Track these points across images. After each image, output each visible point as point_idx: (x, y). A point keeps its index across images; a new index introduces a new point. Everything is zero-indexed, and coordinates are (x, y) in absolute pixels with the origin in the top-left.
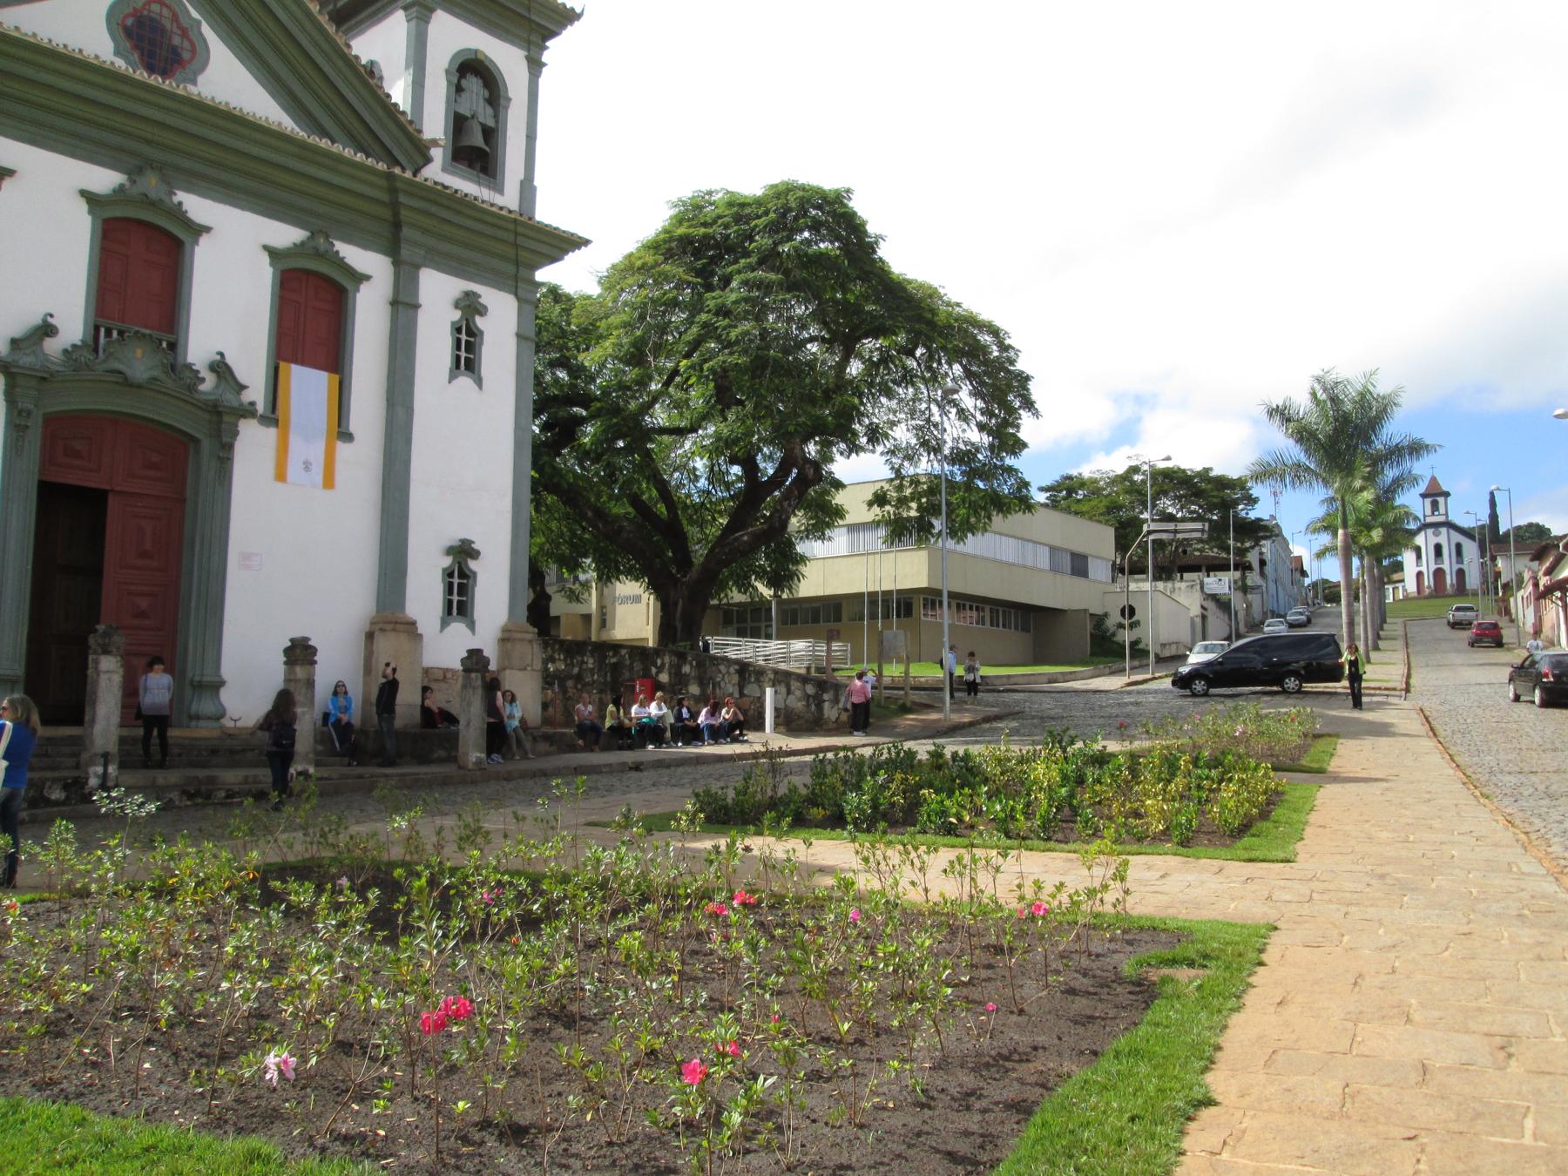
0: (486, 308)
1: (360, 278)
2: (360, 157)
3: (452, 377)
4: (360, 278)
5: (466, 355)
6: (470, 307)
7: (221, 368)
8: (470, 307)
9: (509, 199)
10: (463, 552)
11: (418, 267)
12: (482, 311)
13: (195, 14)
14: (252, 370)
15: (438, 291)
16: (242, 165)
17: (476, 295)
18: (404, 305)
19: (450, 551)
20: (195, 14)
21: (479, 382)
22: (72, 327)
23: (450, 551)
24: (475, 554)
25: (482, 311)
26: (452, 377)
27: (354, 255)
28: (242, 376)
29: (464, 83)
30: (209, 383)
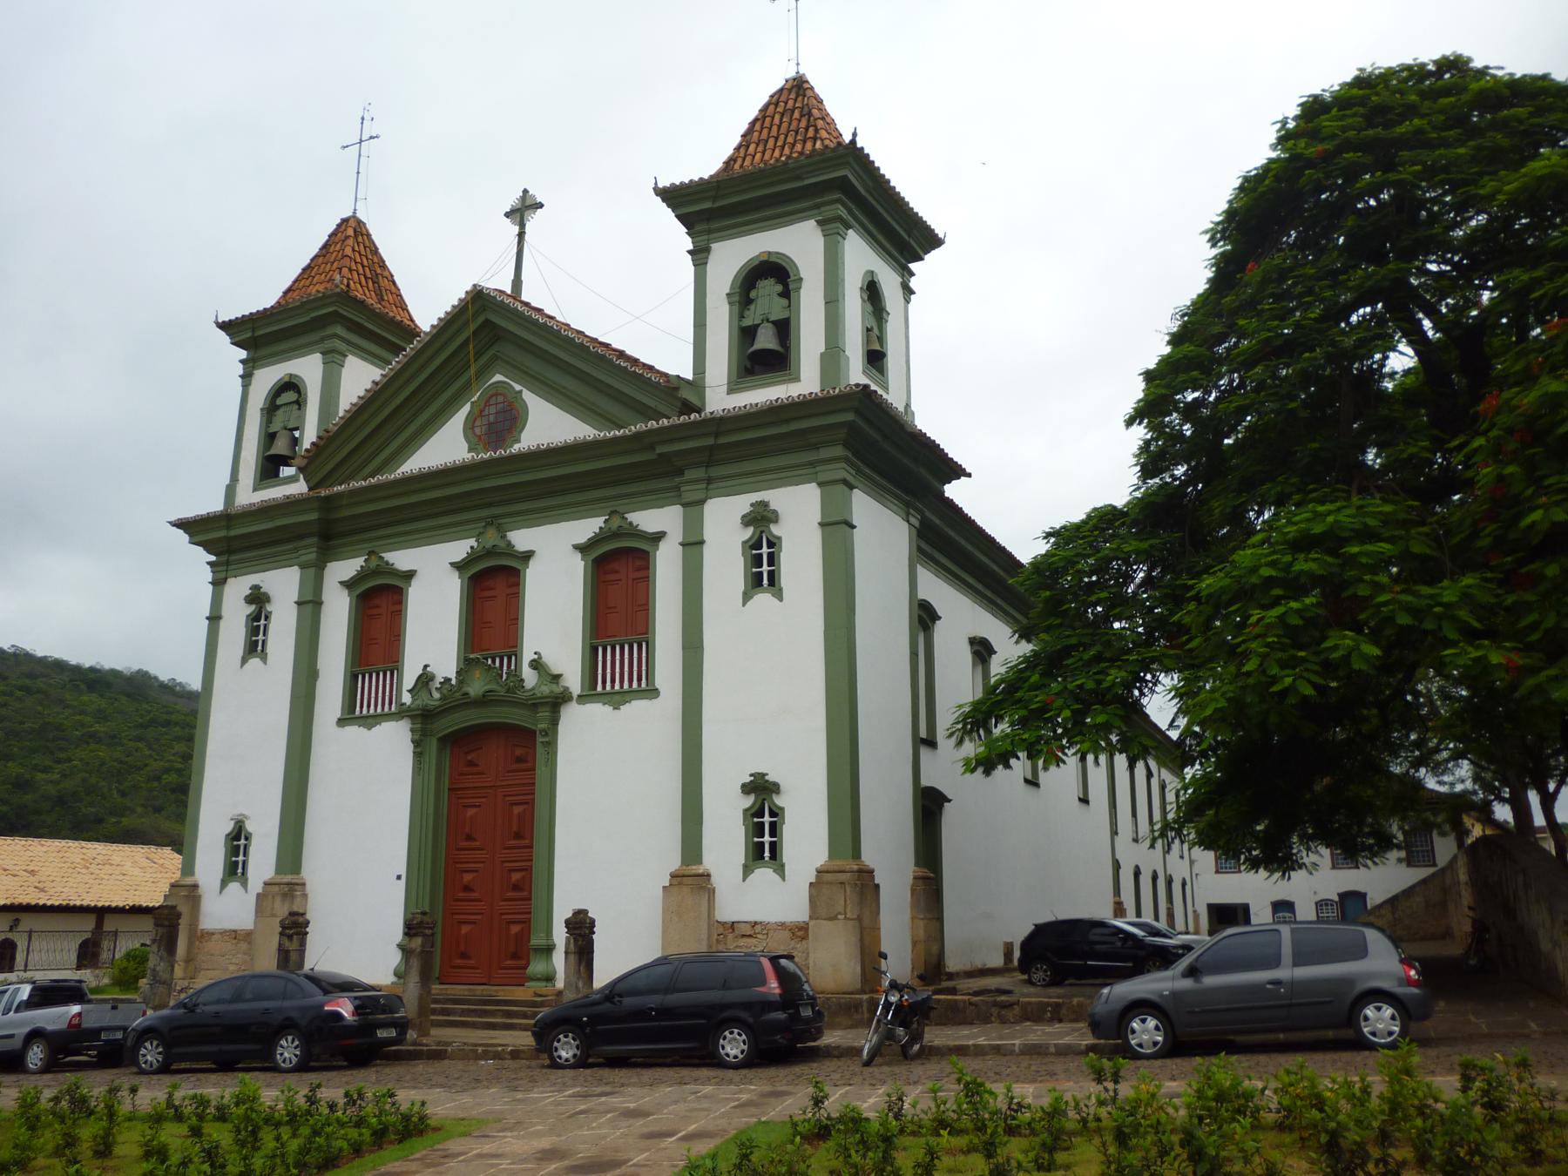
0: (775, 512)
1: (658, 537)
2: (652, 424)
3: (747, 597)
4: (658, 537)
5: (762, 571)
6: (761, 518)
7: (537, 664)
8: (761, 518)
9: (808, 382)
10: (761, 789)
11: (702, 502)
12: (773, 517)
13: (518, 387)
14: (568, 661)
15: (724, 518)
16: (553, 484)
17: (764, 504)
18: (693, 545)
19: (747, 789)
20: (518, 387)
22: (446, 666)
23: (747, 789)
24: (774, 788)
25: (773, 517)
26: (747, 597)
27: (647, 519)
28: (555, 663)
29: (753, 294)
30: (529, 677)
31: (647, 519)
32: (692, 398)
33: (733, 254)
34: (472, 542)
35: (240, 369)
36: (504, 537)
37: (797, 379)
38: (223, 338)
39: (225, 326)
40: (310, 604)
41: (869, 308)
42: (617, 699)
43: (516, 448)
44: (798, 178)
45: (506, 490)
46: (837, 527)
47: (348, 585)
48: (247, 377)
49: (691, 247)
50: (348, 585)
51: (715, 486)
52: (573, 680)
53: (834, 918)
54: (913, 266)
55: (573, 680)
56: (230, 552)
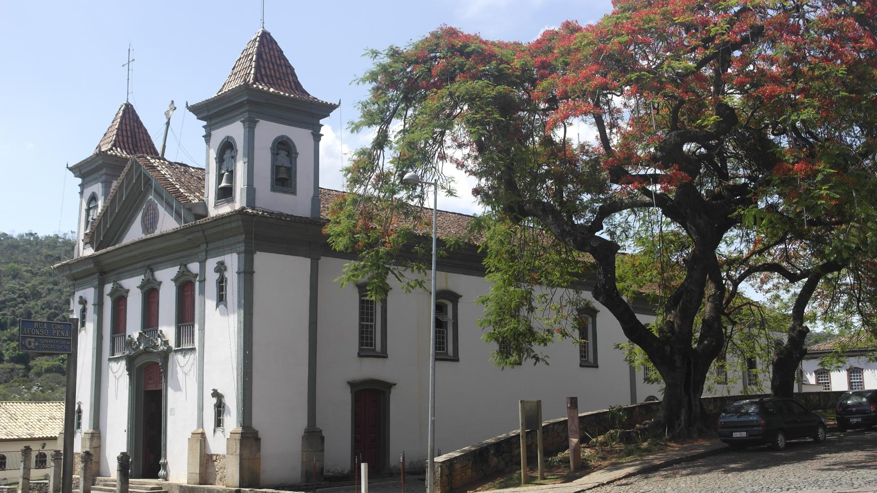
6: (221, 268)
8: (221, 268)
21: (226, 306)
31: (194, 267)
32: (200, 211)
33: (219, 135)
34: (142, 277)
35: (79, 189)
36: (153, 275)
37: (232, 200)
38: (71, 174)
39: (71, 169)
40: (99, 305)
41: (283, 153)
42: (185, 352)
43: (157, 233)
44: (232, 101)
45: (149, 255)
46: (247, 273)
47: (111, 295)
48: (81, 193)
49: (204, 133)
50: (111, 295)
51: (208, 254)
52: (172, 344)
53: (232, 454)
54: (321, 122)
55: (172, 344)
56: (75, 280)
